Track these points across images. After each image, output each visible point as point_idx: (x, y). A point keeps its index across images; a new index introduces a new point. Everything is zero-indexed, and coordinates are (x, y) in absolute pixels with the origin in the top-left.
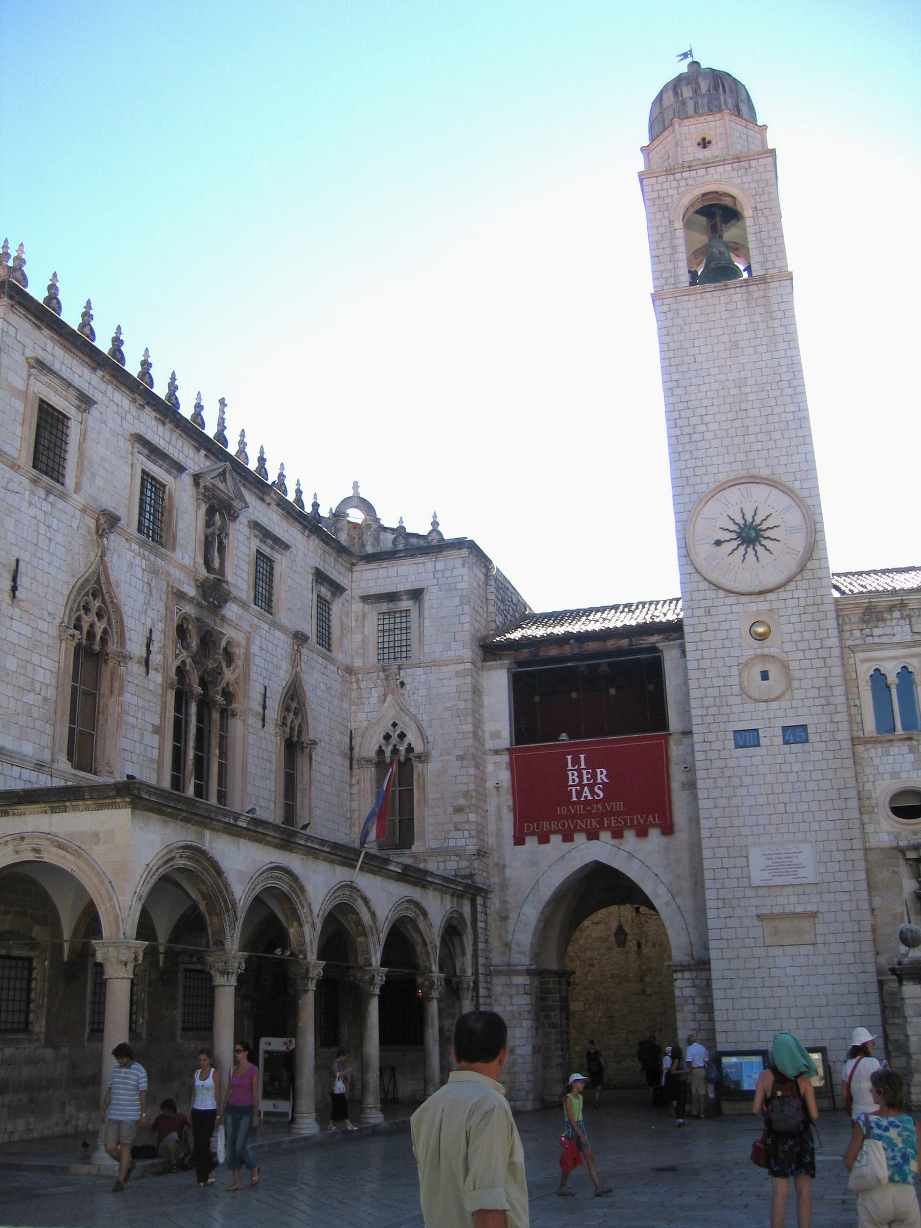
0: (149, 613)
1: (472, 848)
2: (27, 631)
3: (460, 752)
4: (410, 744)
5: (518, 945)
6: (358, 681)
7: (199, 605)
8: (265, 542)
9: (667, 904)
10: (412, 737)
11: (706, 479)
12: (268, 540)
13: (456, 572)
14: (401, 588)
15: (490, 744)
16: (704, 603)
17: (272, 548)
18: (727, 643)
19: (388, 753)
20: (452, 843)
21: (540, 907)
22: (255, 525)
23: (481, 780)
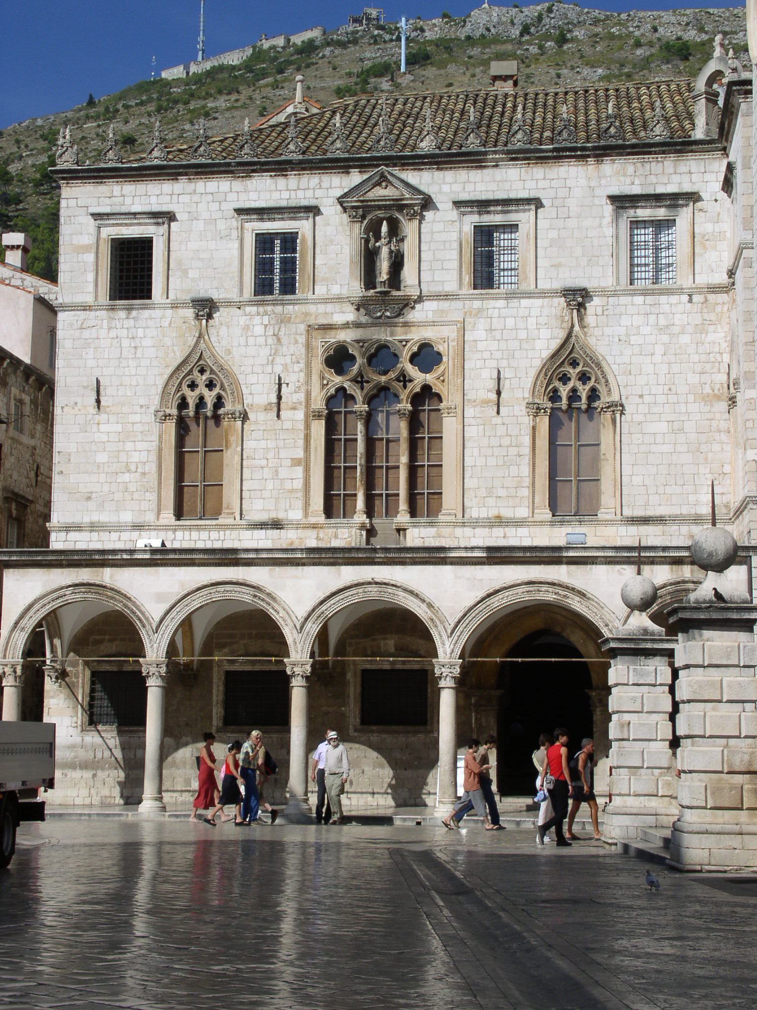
0: (279, 360)
7: (357, 325)
8: (488, 212)
12: (492, 208)
22: (458, 204)
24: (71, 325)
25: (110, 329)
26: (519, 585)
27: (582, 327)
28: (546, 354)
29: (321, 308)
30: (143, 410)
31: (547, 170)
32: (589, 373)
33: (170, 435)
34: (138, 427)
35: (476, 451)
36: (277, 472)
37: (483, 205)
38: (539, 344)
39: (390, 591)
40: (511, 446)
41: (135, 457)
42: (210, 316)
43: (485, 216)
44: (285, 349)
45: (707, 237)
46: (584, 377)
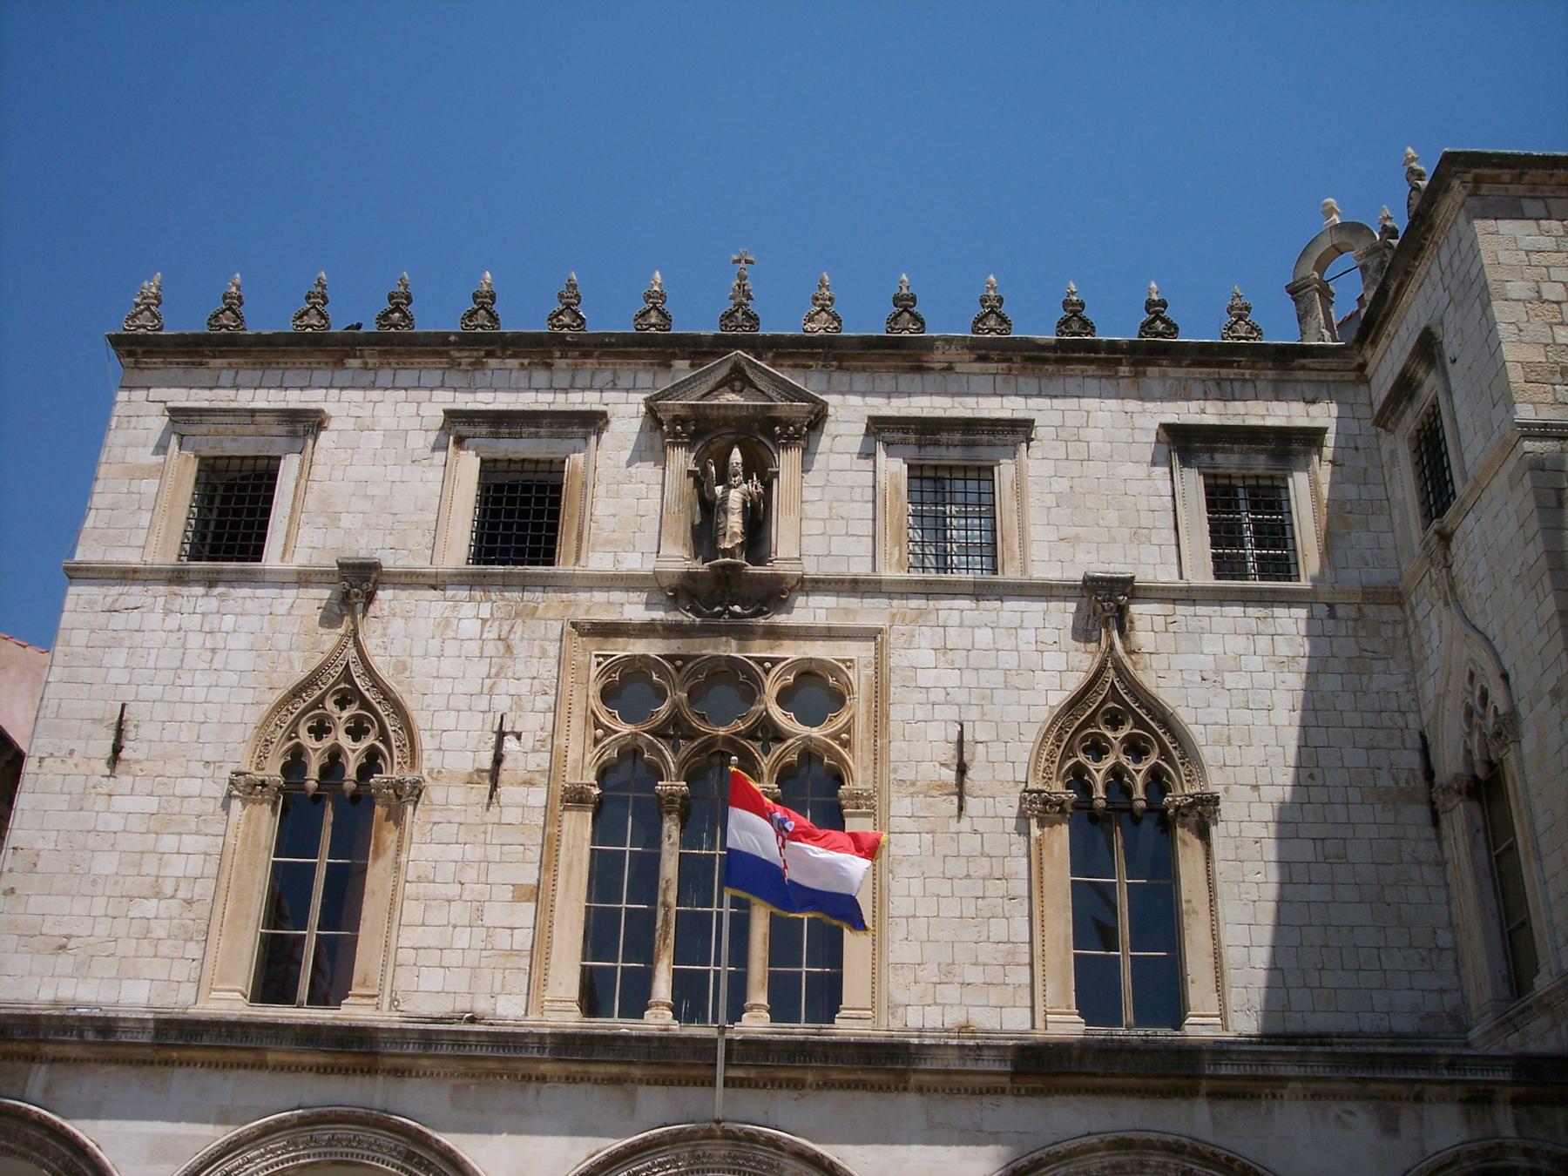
0: (503, 685)
8: (937, 444)
12: (944, 437)
17: (966, 445)
19: (1477, 756)
22: (878, 427)
24: (91, 603)
25: (168, 612)
26: (1092, 1149)
27: (1130, 652)
28: (1059, 698)
29: (599, 596)
30: (208, 772)
31: (1044, 381)
32: (1146, 740)
33: (258, 825)
34: (193, 806)
35: (916, 885)
36: (480, 910)
37: (928, 429)
39: (761, 1156)
40: (990, 877)
41: (177, 866)
42: (370, 598)
43: (930, 449)
44: (519, 667)
45: (1348, 507)
46: (1135, 748)
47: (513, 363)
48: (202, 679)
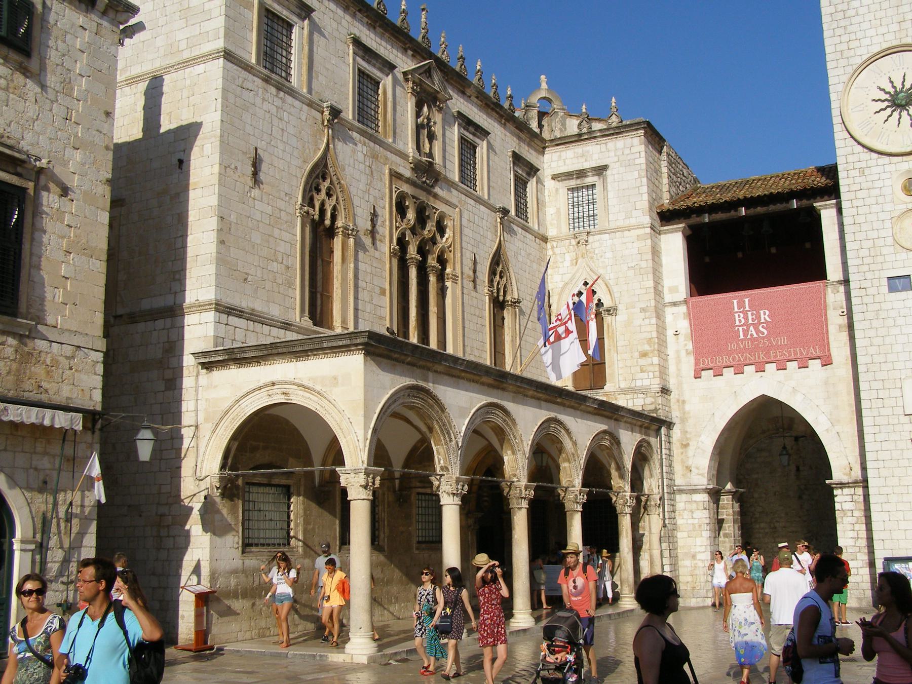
1: (656, 386)
2: (269, 209)
3: (643, 306)
4: (599, 300)
5: (697, 468)
6: (553, 248)
8: (468, 130)
9: (827, 430)
10: (602, 294)
11: (859, 52)
13: (634, 150)
14: (586, 165)
15: (668, 298)
16: (858, 165)
17: (474, 135)
18: (881, 200)
20: (639, 383)
21: (715, 436)
23: (661, 329)
38: (488, 243)
47: (365, 20)
48: (281, 146)
